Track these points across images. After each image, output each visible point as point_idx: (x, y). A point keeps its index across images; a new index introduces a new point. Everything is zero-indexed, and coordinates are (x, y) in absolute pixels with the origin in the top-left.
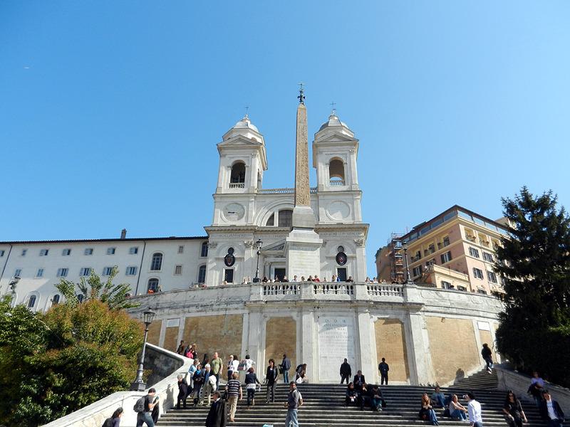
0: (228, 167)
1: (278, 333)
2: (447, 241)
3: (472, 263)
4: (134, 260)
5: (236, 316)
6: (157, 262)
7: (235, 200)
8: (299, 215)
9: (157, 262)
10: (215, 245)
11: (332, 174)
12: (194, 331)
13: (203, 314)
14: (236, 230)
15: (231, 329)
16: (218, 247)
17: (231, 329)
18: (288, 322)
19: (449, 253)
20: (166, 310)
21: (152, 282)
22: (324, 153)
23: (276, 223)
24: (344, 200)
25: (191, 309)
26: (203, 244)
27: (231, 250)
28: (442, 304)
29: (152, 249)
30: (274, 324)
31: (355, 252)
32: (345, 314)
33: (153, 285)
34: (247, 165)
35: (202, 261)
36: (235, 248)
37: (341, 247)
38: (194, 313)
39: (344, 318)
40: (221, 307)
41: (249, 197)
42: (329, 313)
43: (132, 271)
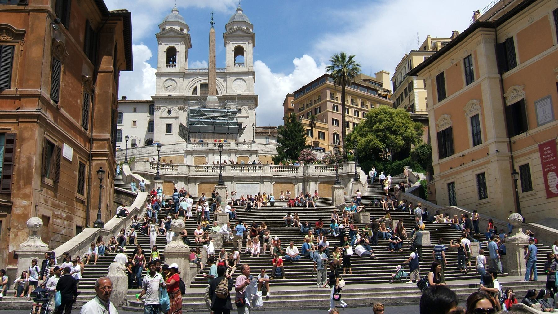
2: (320, 100)
3: (330, 116)
10: (159, 109)
11: (236, 55)
15: (179, 161)
17: (179, 161)
18: (203, 158)
19: (320, 107)
23: (198, 94)
26: (150, 106)
27: (169, 112)
28: (266, 150)
30: (197, 159)
34: (177, 50)
36: (173, 111)
40: (175, 152)
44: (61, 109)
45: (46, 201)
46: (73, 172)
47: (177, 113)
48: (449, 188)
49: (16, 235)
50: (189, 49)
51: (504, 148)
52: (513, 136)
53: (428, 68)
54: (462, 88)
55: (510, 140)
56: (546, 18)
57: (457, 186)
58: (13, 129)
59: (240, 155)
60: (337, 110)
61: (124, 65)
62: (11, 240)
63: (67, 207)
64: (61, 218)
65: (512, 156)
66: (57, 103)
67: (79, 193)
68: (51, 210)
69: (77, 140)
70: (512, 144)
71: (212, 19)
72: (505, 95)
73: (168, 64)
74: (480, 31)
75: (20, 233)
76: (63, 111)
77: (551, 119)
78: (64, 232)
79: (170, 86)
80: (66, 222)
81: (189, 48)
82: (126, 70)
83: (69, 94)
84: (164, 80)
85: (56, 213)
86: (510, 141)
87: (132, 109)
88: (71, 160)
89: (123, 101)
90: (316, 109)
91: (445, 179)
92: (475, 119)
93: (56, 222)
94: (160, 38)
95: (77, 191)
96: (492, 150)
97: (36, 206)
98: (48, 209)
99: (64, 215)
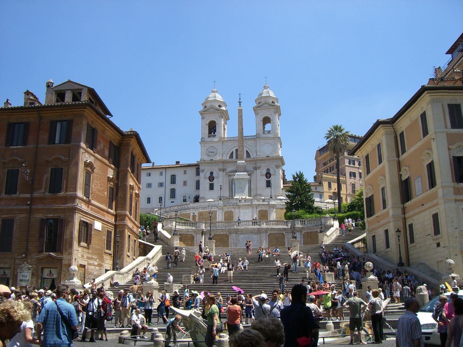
0: (206, 125)
1: (228, 216)
4: (162, 179)
5: (214, 211)
6: (173, 180)
7: (212, 145)
8: (239, 165)
9: (173, 179)
10: (203, 171)
12: (201, 216)
13: (204, 211)
14: (213, 162)
16: (205, 171)
20: (191, 210)
21: (172, 190)
22: (260, 114)
24: (270, 143)
25: (200, 209)
26: (197, 169)
27: (212, 173)
28: (282, 204)
29: (170, 173)
31: (275, 172)
32: (249, 209)
33: (173, 192)
35: (197, 178)
37: (268, 169)
38: (201, 210)
39: (248, 210)
41: (219, 143)
42: (244, 209)
43: (161, 185)
44: (92, 201)
45: (83, 256)
46: (102, 237)
47: (218, 174)
48: (373, 238)
49: (65, 275)
50: (227, 121)
51: (399, 211)
52: (405, 203)
53: (360, 150)
54: (376, 167)
55: (404, 206)
56: (417, 119)
57: (377, 238)
58: (62, 216)
59: (260, 209)
60: (354, 164)
61: (144, 160)
62: (62, 278)
63: (98, 258)
64: (94, 265)
65: (405, 217)
66: (88, 198)
67: (107, 249)
68: (86, 261)
69: (105, 217)
70: (405, 209)
71: (240, 99)
72: (401, 173)
73: (210, 135)
74: (381, 127)
75: (66, 274)
76: (93, 202)
77: (421, 192)
78: (96, 273)
79: (212, 152)
80: (97, 268)
81: (227, 120)
82: (146, 163)
83: (98, 190)
84: (207, 147)
85: (90, 262)
86: (404, 207)
87: (183, 172)
88: (101, 230)
89: (177, 166)
90: (330, 167)
91: (371, 233)
92: (383, 189)
93: (90, 267)
94: (203, 115)
95: (105, 248)
96: (391, 213)
97: (76, 259)
98: (84, 260)
99: (96, 264)
